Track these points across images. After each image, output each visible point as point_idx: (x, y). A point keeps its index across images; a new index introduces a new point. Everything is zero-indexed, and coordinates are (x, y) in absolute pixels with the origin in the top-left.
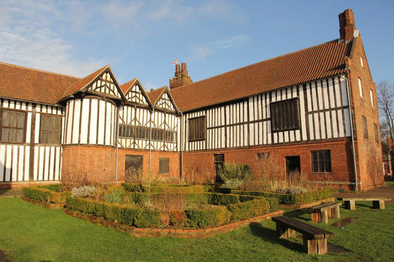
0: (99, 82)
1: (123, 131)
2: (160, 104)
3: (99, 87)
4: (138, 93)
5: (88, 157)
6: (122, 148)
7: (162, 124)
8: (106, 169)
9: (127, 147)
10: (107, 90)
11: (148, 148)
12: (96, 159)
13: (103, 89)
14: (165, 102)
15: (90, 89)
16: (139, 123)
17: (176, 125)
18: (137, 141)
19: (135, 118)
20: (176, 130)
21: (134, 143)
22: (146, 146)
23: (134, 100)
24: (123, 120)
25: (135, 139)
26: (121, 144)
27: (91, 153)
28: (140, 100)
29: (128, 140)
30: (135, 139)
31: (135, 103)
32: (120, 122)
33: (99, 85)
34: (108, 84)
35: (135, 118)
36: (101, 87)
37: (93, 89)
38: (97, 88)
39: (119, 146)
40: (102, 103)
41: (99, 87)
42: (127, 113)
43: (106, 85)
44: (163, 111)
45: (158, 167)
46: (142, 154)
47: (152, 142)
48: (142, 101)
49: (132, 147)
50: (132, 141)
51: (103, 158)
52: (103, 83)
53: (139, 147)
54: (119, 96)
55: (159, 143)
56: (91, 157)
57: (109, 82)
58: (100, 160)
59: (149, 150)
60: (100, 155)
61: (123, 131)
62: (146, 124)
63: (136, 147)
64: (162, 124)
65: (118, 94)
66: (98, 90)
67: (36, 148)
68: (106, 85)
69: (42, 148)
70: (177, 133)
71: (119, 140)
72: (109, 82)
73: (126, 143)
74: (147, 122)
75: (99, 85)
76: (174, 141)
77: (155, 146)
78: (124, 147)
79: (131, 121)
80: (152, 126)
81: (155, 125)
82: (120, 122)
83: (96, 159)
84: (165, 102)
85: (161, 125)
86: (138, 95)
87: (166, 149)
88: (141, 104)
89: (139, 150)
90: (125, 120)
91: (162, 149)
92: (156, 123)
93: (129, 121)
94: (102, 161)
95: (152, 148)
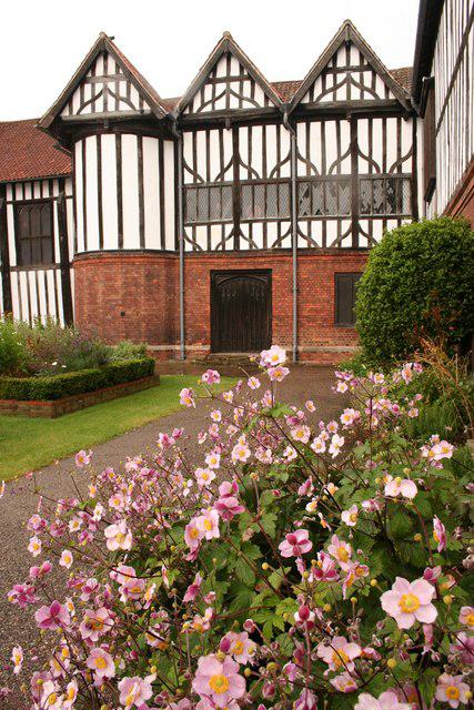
0: (88, 87)
2: (325, 92)
3: (88, 103)
4: (234, 79)
5: (86, 284)
6: (197, 252)
7: (340, 158)
8: (129, 312)
9: (213, 248)
10: (111, 101)
11: (286, 243)
12: (100, 287)
13: (99, 103)
14: (349, 81)
15: (66, 113)
16: (251, 171)
17: (406, 150)
18: (244, 228)
19: (236, 160)
20: (407, 168)
21: (237, 233)
22: (280, 238)
23: (220, 105)
24: (194, 172)
25: (237, 222)
26: (193, 242)
27: (90, 274)
28: (241, 99)
31: (228, 111)
33: (88, 97)
34: (112, 86)
35: (236, 160)
36: (94, 98)
37: (75, 112)
38: (83, 105)
39: (189, 247)
40: (109, 140)
41: (88, 103)
42: (207, 154)
43: (106, 89)
44: (336, 113)
45: (330, 307)
46: (265, 266)
47: (303, 226)
48: (252, 100)
49: (230, 245)
50: (229, 228)
51: (119, 283)
52: (99, 87)
53: (252, 244)
54: (146, 107)
55: (332, 225)
56: (92, 283)
57: (112, 78)
58: (111, 290)
59: (290, 250)
60: (109, 279)
61: (187, 202)
62: (277, 169)
63: (244, 245)
64: (340, 158)
65: (141, 105)
66: (87, 110)
67: (13, 275)
68: (106, 89)
69: (23, 274)
70: (413, 179)
71: (189, 230)
72: (112, 78)
74: (280, 163)
75: (88, 97)
76: (406, 209)
77: (317, 237)
78: (205, 248)
79: (223, 170)
80: (302, 171)
81: (310, 166)
82: (189, 179)
83: (100, 287)
84: (349, 81)
85: (337, 163)
86: (235, 86)
87: (363, 242)
88: (252, 110)
89: (252, 253)
90: (202, 172)
91: (347, 243)
92: (316, 159)
94: (116, 292)
95: (303, 244)
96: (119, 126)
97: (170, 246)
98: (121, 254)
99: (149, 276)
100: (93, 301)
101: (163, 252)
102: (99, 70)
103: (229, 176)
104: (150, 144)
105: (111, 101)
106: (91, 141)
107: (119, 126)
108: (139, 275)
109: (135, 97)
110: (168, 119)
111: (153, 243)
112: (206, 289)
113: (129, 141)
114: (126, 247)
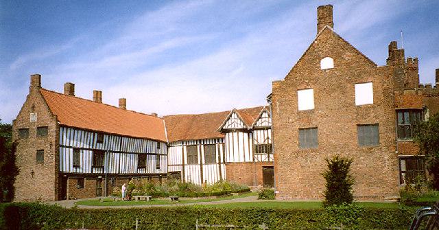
1: (259, 149)
10: (236, 125)
19: (268, 138)
21: (269, 156)
23: (263, 125)
25: (269, 154)
29: (263, 156)
30: (269, 154)
32: (256, 143)
33: (230, 123)
39: (256, 161)
40: (235, 134)
49: (267, 160)
73: (263, 157)
82: (256, 143)
93: (263, 141)
97: (252, 161)
103: (266, 143)
104: (246, 135)
105: (236, 125)
106: (231, 134)
110: (251, 130)
111: (247, 160)
112: (261, 172)
113: (241, 134)
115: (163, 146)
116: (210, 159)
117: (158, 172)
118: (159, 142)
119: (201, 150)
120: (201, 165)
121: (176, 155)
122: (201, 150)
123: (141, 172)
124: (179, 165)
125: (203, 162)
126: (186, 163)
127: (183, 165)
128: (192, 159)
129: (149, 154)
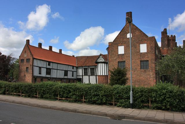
12: (100, 79)
40: (101, 64)
60: (101, 78)
83: (100, 79)
96: (102, 63)
97: (107, 75)
98: (102, 76)
99: (105, 78)
100: (100, 80)
101: (107, 75)
102: (100, 57)
106: (99, 64)
107: (102, 63)
108: (104, 78)
109: (104, 60)
111: (106, 74)
113: (103, 64)
114: (103, 75)
115: (74, 68)
116: (93, 74)
117: (72, 78)
118: (73, 67)
119: (89, 71)
120: (89, 76)
121: (80, 72)
122: (89, 71)
123: (66, 77)
124: (81, 76)
125: (90, 75)
126: (83, 75)
127: (82, 76)
128: (86, 74)
129: (69, 71)
